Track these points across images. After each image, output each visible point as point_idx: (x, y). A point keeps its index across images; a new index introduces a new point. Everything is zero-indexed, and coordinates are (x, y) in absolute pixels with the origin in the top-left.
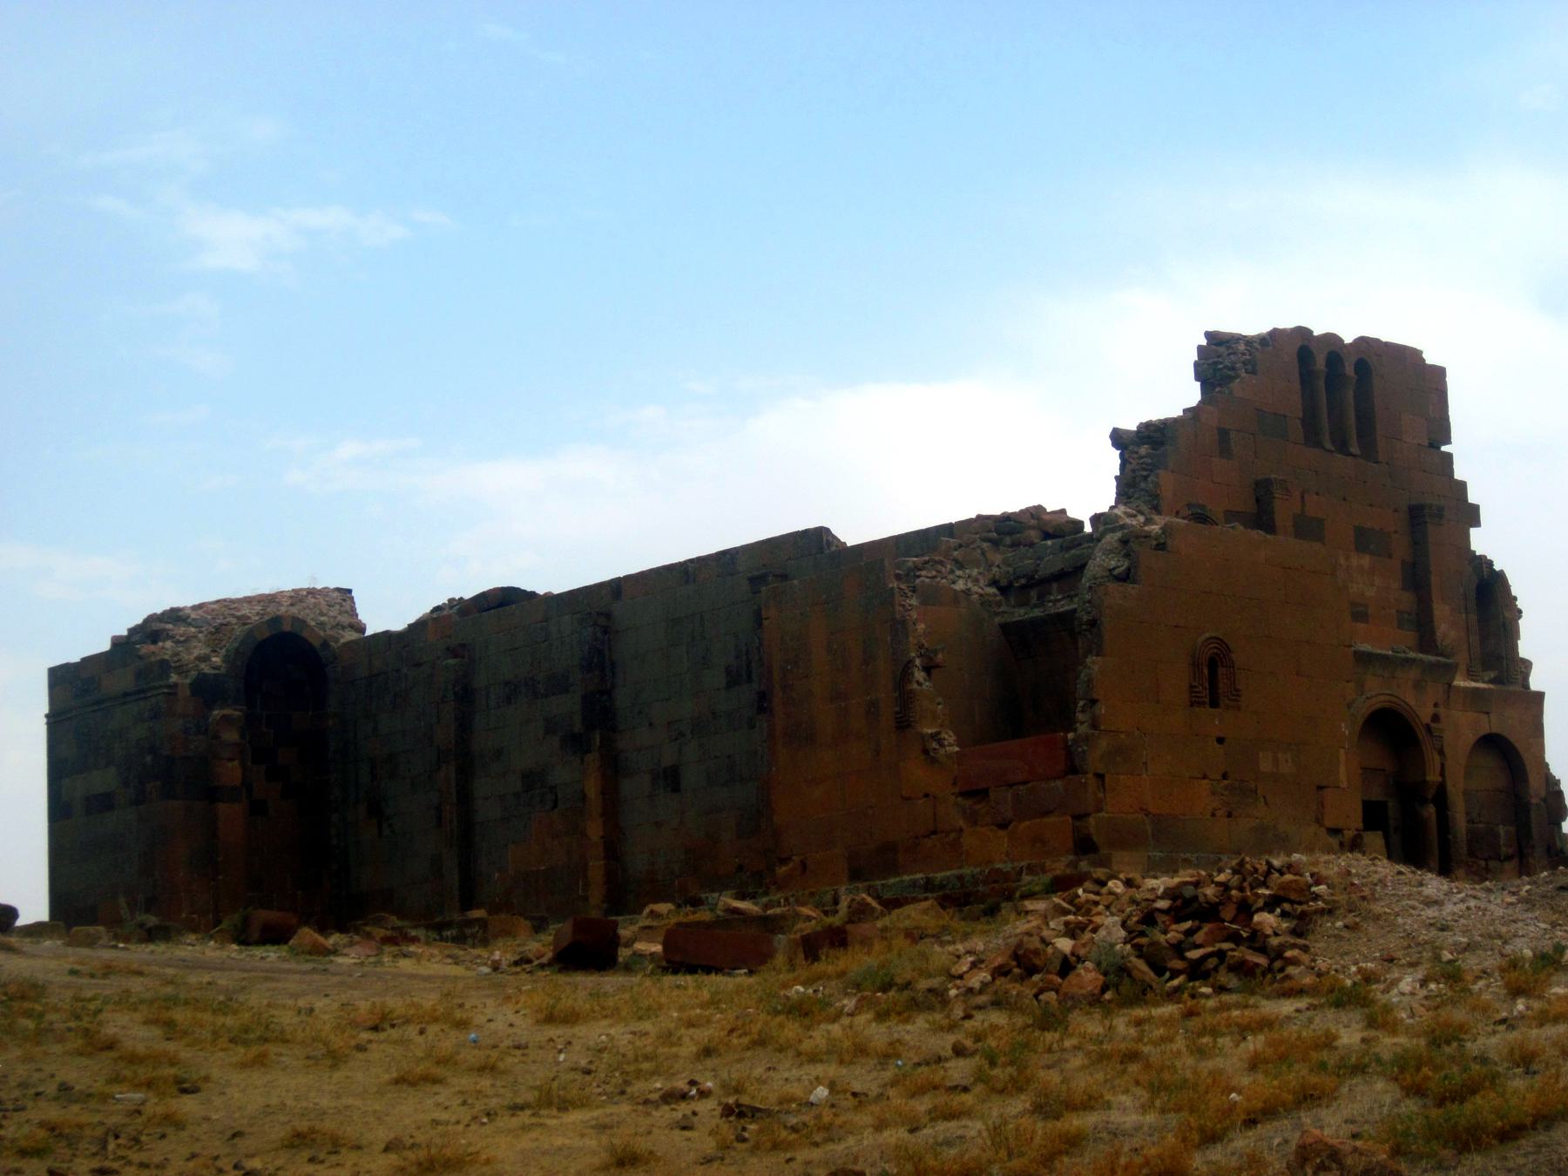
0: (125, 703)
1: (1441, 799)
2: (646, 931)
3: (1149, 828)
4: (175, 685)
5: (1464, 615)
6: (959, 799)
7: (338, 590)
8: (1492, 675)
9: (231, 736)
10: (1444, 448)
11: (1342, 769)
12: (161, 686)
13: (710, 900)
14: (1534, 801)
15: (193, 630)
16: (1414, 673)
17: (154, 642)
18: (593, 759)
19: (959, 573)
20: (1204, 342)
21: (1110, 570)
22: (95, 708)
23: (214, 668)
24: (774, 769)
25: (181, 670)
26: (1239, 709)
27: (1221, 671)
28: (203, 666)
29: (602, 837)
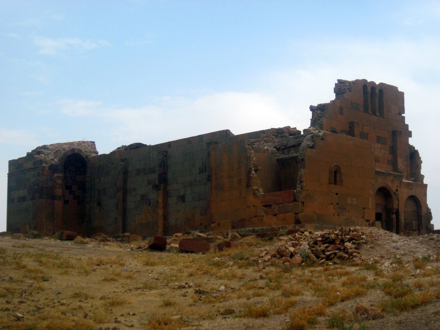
0: (30, 171)
1: (397, 213)
2: (175, 241)
3: (316, 218)
4: (44, 167)
5: (406, 162)
6: (263, 207)
7: (91, 142)
8: (413, 179)
9: (60, 182)
10: (403, 115)
11: (370, 204)
12: (40, 167)
13: (192, 233)
14: (423, 214)
15: (50, 151)
16: (391, 178)
17: (39, 154)
18: (161, 192)
19: (265, 144)
20: (337, 82)
21: (308, 145)
22: (21, 172)
23: (56, 162)
25: (46, 162)
26: (342, 185)
27: (338, 175)
28: (52, 162)
29: (163, 214)
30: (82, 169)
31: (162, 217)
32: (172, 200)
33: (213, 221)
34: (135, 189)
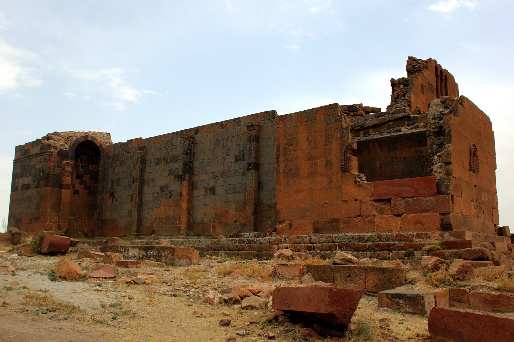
0: (36, 157)
2: (282, 267)
4: (52, 152)
6: (373, 203)
7: (106, 133)
9: (69, 169)
12: (47, 152)
13: (245, 235)
15: (61, 138)
17: (48, 140)
18: (185, 183)
21: (440, 112)
22: (27, 158)
23: (66, 148)
24: (278, 186)
25: (54, 148)
28: (62, 147)
29: (187, 208)
30: (95, 158)
31: (186, 211)
32: (199, 193)
33: (281, 221)
34: (153, 180)
